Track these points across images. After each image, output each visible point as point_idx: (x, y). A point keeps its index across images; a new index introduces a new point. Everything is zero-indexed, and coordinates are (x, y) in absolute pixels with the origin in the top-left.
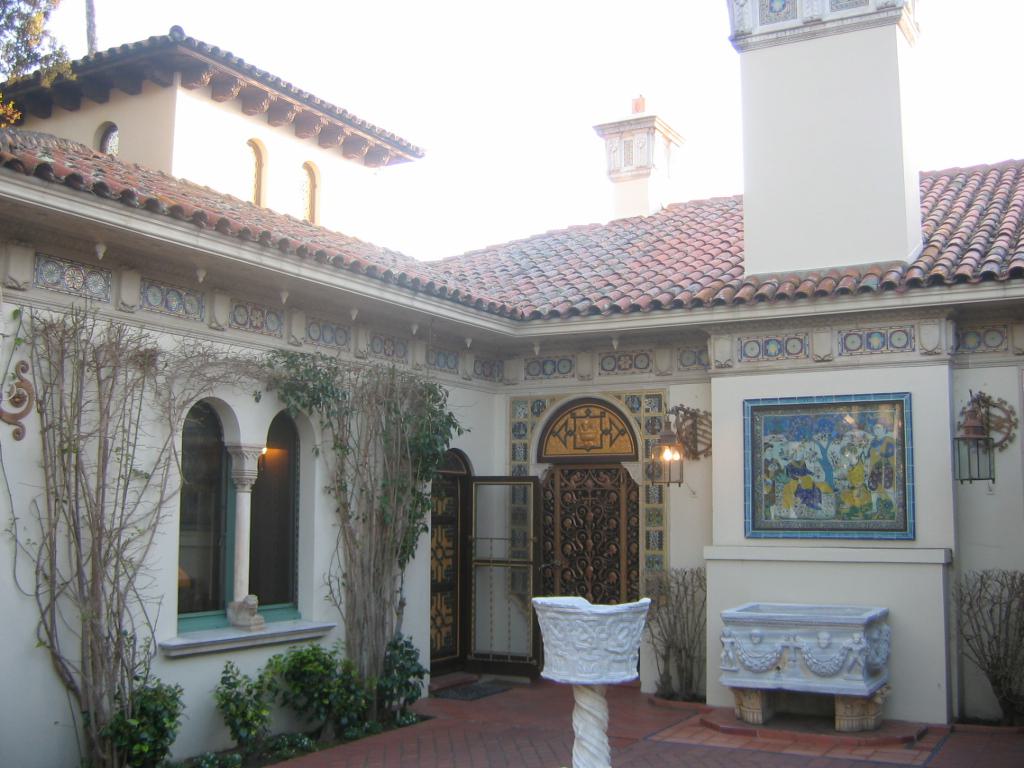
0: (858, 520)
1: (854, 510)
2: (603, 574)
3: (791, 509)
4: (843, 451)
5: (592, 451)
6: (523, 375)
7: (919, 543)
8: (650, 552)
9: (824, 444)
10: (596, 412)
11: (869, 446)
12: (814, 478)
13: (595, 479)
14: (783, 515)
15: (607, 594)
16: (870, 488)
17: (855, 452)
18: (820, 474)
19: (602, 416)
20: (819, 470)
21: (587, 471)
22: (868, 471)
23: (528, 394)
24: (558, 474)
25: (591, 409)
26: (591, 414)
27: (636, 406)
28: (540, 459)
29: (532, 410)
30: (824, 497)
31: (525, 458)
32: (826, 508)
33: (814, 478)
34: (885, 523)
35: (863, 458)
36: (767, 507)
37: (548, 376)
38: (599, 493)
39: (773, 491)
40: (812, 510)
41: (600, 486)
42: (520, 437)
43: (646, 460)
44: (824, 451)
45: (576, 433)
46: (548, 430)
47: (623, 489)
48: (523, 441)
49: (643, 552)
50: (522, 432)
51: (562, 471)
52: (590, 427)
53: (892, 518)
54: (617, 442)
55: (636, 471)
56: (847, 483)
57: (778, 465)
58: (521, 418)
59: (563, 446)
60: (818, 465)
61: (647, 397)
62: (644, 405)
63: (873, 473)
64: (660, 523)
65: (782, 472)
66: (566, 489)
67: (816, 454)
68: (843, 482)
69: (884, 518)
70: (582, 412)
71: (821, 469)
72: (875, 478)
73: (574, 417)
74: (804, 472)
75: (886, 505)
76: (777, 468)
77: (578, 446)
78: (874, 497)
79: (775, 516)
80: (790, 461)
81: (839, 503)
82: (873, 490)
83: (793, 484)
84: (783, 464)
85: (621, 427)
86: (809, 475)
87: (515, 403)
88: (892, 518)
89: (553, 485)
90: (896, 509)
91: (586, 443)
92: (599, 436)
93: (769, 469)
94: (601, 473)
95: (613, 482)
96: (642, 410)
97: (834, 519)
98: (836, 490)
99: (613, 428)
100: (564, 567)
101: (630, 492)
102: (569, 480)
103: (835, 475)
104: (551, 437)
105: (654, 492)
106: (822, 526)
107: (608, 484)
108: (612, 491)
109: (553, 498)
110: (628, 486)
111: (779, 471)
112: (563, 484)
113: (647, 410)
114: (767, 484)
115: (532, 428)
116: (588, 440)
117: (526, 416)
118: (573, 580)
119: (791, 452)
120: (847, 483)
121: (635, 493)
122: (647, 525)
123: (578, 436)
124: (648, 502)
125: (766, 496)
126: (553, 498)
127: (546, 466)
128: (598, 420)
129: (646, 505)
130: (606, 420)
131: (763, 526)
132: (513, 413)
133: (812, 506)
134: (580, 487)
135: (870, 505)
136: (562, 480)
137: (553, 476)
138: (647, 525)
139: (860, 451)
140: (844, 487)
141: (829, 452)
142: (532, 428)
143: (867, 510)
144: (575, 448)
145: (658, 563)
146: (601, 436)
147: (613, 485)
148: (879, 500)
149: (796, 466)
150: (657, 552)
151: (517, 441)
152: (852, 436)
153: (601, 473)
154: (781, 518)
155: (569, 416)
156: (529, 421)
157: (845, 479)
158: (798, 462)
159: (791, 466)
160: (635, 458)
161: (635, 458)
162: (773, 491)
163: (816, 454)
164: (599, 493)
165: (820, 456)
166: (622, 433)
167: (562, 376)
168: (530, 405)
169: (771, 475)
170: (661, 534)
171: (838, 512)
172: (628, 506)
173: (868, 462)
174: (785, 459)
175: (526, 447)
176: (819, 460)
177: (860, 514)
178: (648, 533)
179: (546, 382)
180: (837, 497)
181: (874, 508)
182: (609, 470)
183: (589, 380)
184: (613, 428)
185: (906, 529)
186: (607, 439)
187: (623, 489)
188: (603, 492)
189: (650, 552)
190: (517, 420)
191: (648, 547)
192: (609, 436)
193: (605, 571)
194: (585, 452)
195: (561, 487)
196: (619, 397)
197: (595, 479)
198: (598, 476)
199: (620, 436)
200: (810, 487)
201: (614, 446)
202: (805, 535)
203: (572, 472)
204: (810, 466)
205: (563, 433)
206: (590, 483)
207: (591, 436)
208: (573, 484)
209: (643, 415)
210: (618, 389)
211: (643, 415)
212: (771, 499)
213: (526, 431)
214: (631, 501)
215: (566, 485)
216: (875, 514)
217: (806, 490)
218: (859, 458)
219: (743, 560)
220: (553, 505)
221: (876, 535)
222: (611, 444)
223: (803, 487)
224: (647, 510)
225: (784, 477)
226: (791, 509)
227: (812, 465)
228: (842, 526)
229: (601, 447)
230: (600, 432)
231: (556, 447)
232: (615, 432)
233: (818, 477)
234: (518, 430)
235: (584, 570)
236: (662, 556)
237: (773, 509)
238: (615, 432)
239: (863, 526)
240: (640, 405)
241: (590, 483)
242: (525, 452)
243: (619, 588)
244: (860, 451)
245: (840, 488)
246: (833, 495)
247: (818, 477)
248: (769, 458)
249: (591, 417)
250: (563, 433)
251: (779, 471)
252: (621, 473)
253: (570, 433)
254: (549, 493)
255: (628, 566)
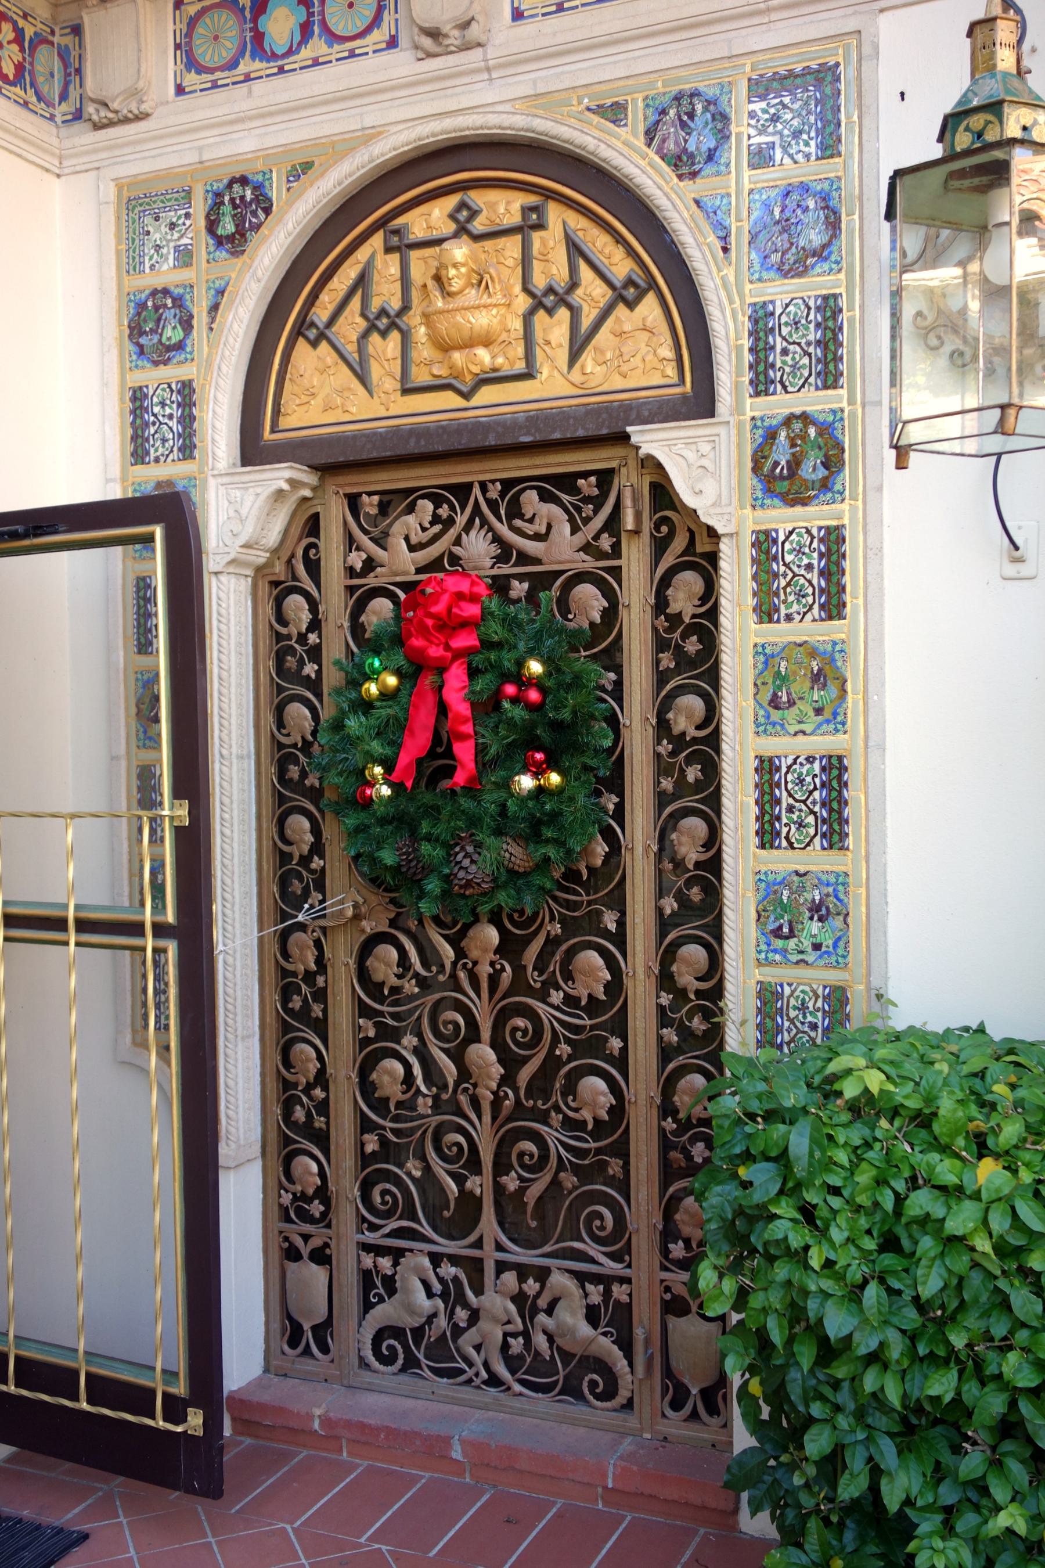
2: (541, 965)
5: (487, 395)
6: (162, 68)
8: (781, 862)
10: (503, 207)
13: (503, 530)
15: (564, 1050)
19: (531, 223)
21: (462, 491)
23: (191, 158)
24: (335, 514)
25: (478, 198)
26: (478, 225)
27: (700, 141)
28: (253, 451)
29: (212, 226)
31: (188, 450)
37: (279, 61)
38: (519, 589)
41: (524, 558)
42: (166, 353)
43: (754, 407)
45: (414, 319)
46: (287, 320)
47: (636, 562)
48: (173, 373)
49: (743, 862)
50: (172, 333)
51: (353, 502)
52: (480, 281)
54: (604, 335)
55: (705, 468)
58: (166, 273)
59: (355, 384)
61: (759, 88)
62: (744, 132)
64: (832, 716)
66: (371, 581)
70: (432, 218)
73: (401, 246)
77: (420, 376)
85: (621, 267)
87: (140, 206)
89: (313, 568)
91: (457, 356)
92: (517, 325)
94: (530, 499)
95: (579, 539)
96: (735, 154)
99: (585, 273)
100: (368, 927)
101: (665, 582)
102: (380, 541)
104: (301, 344)
105: (801, 564)
107: (563, 548)
108: (580, 577)
109: (315, 625)
110: (660, 547)
112: (357, 560)
113: (761, 158)
115: (215, 308)
116: (468, 344)
117: (185, 257)
118: (411, 987)
121: (690, 582)
122: (764, 727)
123: (421, 332)
124: (766, 613)
126: (315, 625)
127: (279, 475)
128: (512, 246)
129: (757, 632)
130: (550, 243)
132: (132, 259)
134: (435, 565)
136: (351, 543)
137: (313, 526)
138: (764, 727)
142: (215, 308)
144: (406, 391)
145: (819, 911)
146: (528, 318)
147: (586, 548)
150: (817, 860)
151: (152, 377)
153: (530, 499)
155: (377, 241)
156: (197, 279)
160: (700, 403)
161: (700, 403)
164: (519, 589)
166: (625, 295)
167: (340, 49)
168: (200, 208)
170: (835, 769)
172: (661, 645)
175: (186, 392)
178: (767, 767)
179: (270, 90)
182: (567, 482)
183: (466, 47)
184: (585, 273)
186: (555, 330)
187: (636, 562)
188: (541, 581)
189: (781, 862)
190: (151, 281)
191: (768, 835)
192: (563, 314)
193: (552, 942)
194: (450, 400)
195: (351, 572)
196: (614, 112)
197: (503, 530)
198: (515, 511)
199: (621, 310)
201: (588, 359)
203: (393, 502)
205: (350, 327)
206: (478, 548)
207: (491, 326)
208: (401, 561)
209: (742, 187)
210: (605, 71)
211: (742, 187)
213: (187, 324)
214: (675, 619)
215: (370, 565)
220: (315, 653)
222: (574, 356)
224: (760, 650)
229: (528, 375)
230: (523, 302)
231: (322, 396)
232: (592, 292)
234: (153, 325)
235: (458, 1056)
236: (841, 881)
238: (592, 292)
240: (723, 136)
241: (478, 548)
242: (188, 420)
243: (620, 1027)
249: (477, 238)
250: (350, 327)
252: (630, 484)
253: (386, 322)
254: (296, 600)
255: (664, 924)
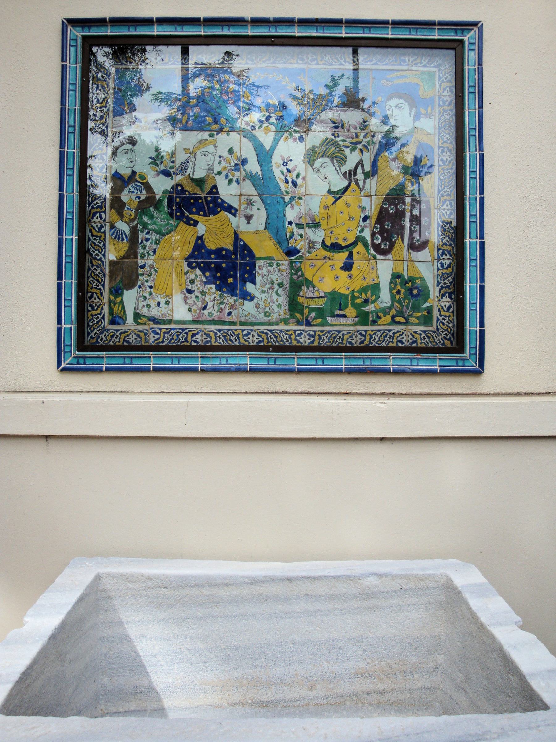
0: (345, 326)
1: (337, 301)
3: (178, 298)
4: (311, 156)
7: (491, 379)
9: (267, 140)
11: (373, 149)
12: (237, 222)
14: (155, 312)
16: (377, 248)
17: (342, 161)
18: (254, 211)
20: (250, 203)
22: (372, 207)
30: (262, 271)
32: (264, 301)
33: (237, 222)
34: (412, 331)
35: (360, 176)
36: (117, 292)
39: (132, 253)
40: (229, 299)
44: (264, 156)
53: (427, 319)
56: (318, 236)
57: (148, 187)
60: (248, 188)
63: (382, 216)
65: (157, 205)
67: (244, 162)
68: (309, 233)
69: (407, 323)
71: (256, 199)
72: (388, 226)
74: (213, 204)
75: (409, 289)
76: (144, 195)
78: (385, 269)
79: (137, 316)
80: (178, 178)
81: (296, 286)
82: (384, 253)
83: (180, 241)
84: (161, 186)
86: (224, 214)
88: (427, 319)
90: (438, 302)
93: (125, 197)
97: (286, 322)
98: (291, 252)
103: (291, 214)
106: (254, 340)
111: (149, 203)
114: (118, 235)
119: (181, 158)
120: (318, 236)
125: (112, 263)
131: (103, 339)
133: (232, 290)
135: (376, 288)
139: (352, 159)
140: (311, 245)
141: (276, 159)
143: (366, 301)
148: (396, 276)
149: (191, 188)
152: (337, 126)
154: (154, 320)
157: (315, 225)
158: (200, 182)
159: (178, 188)
162: (132, 253)
163: (244, 162)
165: (253, 167)
169: (128, 213)
171: (294, 306)
173: (372, 185)
174: (167, 174)
176: (251, 177)
177: (350, 312)
180: (294, 269)
181: (385, 297)
185: (459, 347)
200: (228, 244)
202: (166, 363)
204: (228, 192)
212: (127, 275)
216: (386, 311)
217: (218, 252)
218: (350, 175)
219: (47, 437)
221: (393, 362)
223: (211, 245)
225: (160, 218)
226: (178, 298)
227: (234, 189)
228: (305, 341)
233: (249, 218)
237: (130, 298)
239: (357, 341)
244: (352, 159)
245: (301, 245)
246: (285, 264)
247: (249, 218)
248: (126, 172)
251: (149, 203)
